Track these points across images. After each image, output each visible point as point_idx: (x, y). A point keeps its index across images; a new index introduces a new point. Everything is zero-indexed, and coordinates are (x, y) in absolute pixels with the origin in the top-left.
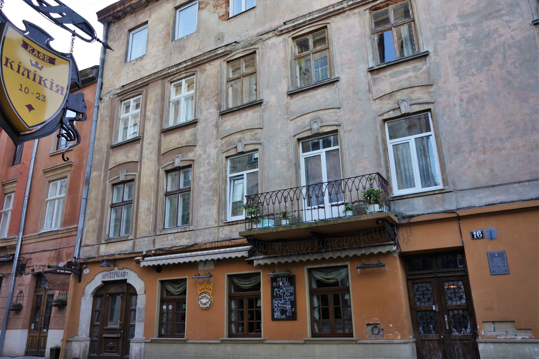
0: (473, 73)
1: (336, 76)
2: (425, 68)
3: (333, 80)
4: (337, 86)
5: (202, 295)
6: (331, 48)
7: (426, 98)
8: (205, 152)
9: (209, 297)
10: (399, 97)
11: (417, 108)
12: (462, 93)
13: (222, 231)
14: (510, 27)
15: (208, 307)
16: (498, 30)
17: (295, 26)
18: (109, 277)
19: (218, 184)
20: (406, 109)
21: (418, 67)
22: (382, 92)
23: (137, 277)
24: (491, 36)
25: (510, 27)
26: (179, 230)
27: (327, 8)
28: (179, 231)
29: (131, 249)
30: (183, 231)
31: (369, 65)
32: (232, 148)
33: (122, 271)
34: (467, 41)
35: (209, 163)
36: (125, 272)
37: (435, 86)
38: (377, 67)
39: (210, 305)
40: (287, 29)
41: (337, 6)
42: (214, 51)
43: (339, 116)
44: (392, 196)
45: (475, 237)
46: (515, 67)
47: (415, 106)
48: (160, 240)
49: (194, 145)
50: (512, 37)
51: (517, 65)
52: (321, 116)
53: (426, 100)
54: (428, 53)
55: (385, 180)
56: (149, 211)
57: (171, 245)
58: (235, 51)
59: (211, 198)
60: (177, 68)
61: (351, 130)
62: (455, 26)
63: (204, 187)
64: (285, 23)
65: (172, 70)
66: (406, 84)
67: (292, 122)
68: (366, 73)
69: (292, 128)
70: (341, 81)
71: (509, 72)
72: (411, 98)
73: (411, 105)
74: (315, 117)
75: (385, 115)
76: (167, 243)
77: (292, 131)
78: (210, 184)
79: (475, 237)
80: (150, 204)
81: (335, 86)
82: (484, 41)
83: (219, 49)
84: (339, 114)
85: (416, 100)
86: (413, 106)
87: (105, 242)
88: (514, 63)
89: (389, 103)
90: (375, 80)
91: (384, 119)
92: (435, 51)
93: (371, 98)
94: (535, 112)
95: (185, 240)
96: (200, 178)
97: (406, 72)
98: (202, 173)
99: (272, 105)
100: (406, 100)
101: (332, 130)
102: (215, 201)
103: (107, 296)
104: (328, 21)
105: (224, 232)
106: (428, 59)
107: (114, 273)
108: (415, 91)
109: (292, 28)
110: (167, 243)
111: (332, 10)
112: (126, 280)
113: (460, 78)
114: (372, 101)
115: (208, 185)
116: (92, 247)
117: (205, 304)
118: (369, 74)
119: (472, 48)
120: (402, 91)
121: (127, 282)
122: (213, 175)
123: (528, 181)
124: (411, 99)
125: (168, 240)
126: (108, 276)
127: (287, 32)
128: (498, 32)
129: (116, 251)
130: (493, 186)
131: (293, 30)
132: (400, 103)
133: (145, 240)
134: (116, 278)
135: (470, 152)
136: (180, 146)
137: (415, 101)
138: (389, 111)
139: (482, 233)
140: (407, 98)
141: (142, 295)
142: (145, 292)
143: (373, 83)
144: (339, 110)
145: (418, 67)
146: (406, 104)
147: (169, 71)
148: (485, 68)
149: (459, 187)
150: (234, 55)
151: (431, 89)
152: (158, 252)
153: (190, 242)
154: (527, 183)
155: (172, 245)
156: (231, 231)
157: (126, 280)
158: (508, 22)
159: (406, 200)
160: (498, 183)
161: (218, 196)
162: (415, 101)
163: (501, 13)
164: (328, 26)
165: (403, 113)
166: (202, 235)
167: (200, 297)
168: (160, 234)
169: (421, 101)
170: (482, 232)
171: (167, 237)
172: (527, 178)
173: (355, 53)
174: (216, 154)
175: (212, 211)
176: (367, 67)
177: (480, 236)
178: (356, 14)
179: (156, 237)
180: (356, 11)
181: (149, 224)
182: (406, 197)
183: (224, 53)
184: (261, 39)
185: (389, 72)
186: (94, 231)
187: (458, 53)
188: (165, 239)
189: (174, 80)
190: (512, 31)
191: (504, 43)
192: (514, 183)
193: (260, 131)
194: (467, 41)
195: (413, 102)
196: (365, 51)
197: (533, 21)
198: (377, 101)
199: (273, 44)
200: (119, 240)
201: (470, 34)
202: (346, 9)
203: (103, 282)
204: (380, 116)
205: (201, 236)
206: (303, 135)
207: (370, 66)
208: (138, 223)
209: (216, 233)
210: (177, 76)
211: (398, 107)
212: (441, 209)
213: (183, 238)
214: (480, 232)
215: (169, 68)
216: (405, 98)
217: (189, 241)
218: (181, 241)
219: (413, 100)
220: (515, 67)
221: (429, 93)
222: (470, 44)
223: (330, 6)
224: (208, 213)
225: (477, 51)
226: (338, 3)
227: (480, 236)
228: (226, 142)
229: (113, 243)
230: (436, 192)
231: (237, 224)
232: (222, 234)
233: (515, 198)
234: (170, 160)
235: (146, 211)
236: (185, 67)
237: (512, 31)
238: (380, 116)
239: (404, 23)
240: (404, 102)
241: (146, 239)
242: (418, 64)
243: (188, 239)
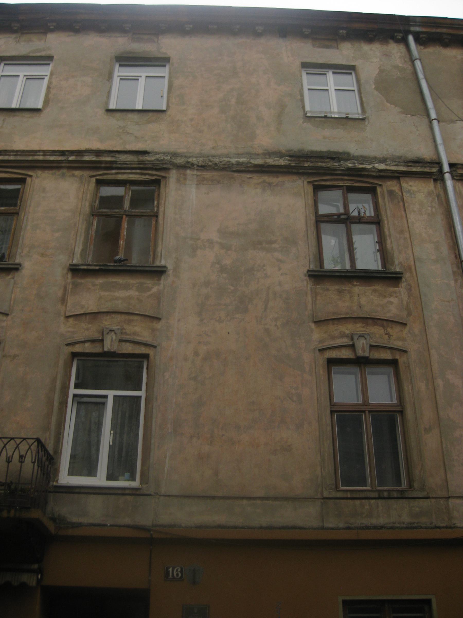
0: (220, 318)
1: (17, 261)
2: (155, 290)
3: (10, 266)
4: (13, 278)
6: (22, 214)
7: (145, 336)
10: (107, 323)
11: (128, 349)
12: (200, 343)
14: (280, 269)
16: (265, 268)
20: (111, 346)
21: (146, 285)
22: (83, 307)
24: (255, 273)
25: (280, 269)
27: (34, 152)
31: (73, 260)
34: (223, 269)
37: (163, 322)
38: (85, 267)
44: (55, 484)
45: (171, 576)
46: (276, 325)
47: (128, 344)
50: (280, 284)
51: (279, 323)
53: (145, 339)
54: (164, 269)
55: (49, 454)
61: (15, 356)
62: (211, 242)
66: (121, 306)
68: (65, 271)
70: (23, 271)
71: (267, 331)
72: (125, 329)
73: (121, 341)
75: (77, 346)
79: (171, 576)
81: (10, 277)
82: (244, 277)
85: (130, 335)
86: (124, 343)
88: (276, 320)
89: (88, 329)
90: (75, 285)
91: (74, 351)
92: (175, 270)
93: (62, 313)
94: (290, 398)
97: (126, 287)
100: (116, 331)
104: (30, 173)
106: (163, 277)
108: (133, 320)
111: (41, 158)
113: (202, 320)
114: (62, 318)
118: (70, 275)
119: (227, 281)
120: (113, 315)
123: (262, 499)
124: (124, 331)
128: (264, 270)
130: (213, 498)
132: (105, 333)
135: (192, 437)
137: (128, 337)
138: (85, 342)
139: (181, 572)
140: (118, 329)
143: (72, 288)
144: (5, 318)
145: (146, 285)
146: (114, 337)
148: (237, 316)
149: (163, 490)
151: (158, 325)
154: (259, 502)
158: (280, 261)
159: (76, 496)
160: (220, 494)
162: (128, 337)
163: (273, 246)
164: (29, 180)
165: (106, 349)
169: (138, 338)
170: (182, 569)
172: (261, 493)
173: (57, 235)
176: (70, 262)
177: (177, 575)
178: (76, 176)
180: (77, 173)
182: (77, 490)
185: (100, 281)
187: (207, 284)
190: (281, 274)
191: (269, 288)
192: (243, 498)
194: (223, 269)
195: (125, 337)
196: (73, 236)
197: (308, 271)
198: (71, 320)
201: (227, 262)
202: (63, 165)
204: (68, 345)
207: (75, 262)
211: (100, 338)
212: (127, 521)
214: (179, 570)
216: (114, 328)
219: (126, 333)
220: (276, 325)
221: (153, 330)
222: (225, 275)
223: (39, 151)
225: (232, 288)
227: (177, 575)
230: (127, 492)
233: (239, 521)
237: (281, 274)
238: (68, 345)
239: (143, 214)
240: (113, 333)
242: (148, 282)
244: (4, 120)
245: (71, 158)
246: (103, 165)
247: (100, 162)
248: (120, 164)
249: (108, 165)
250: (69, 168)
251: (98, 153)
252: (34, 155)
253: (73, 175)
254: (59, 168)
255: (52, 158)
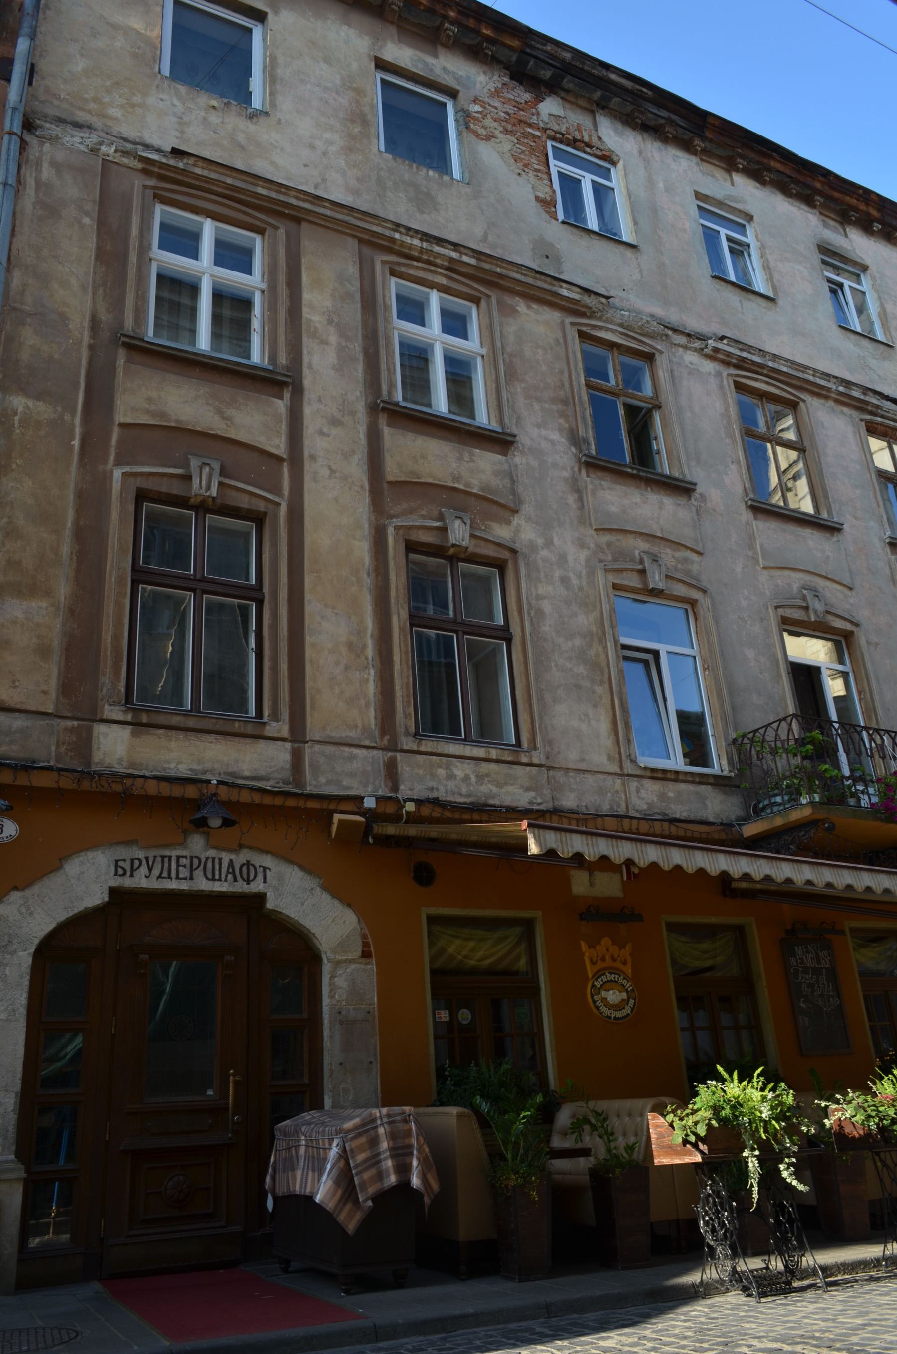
5: (604, 979)
8: (549, 544)
9: (628, 985)
13: (638, 791)
15: (628, 1015)
17: (744, 359)
18: (156, 872)
19: (600, 649)
23: (319, 889)
26: (494, 753)
28: (494, 757)
29: (287, 774)
30: (509, 759)
32: (632, 570)
33: (233, 857)
35: (564, 580)
36: (248, 864)
39: (632, 1009)
40: (728, 356)
41: (819, 377)
42: (549, 280)
43: (851, 605)
48: (421, 772)
49: (512, 505)
52: (820, 590)
56: (358, 656)
57: (466, 796)
58: (600, 319)
59: (586, 684)
60: (425, 245)
61: (876, 644)
63: (559, 645)
64: (722, 338)
65: (408, 240)
67: (766, 572)
69: (766, 587)
74: (809, 584)
76: (451, 785)
77: (767, 592)
78: (577, 642)
80: (360, 632)
81: (835, 539)
83: (564, 285)
84: (851, 601)
87: (129, 718)
95: (521, 791)
96: (540, 612)
98: (546, 600)
99: (714, 510)
101: (844, 628)
102: (601, 698)
103: (144, 957)
105: (643, 793)
107: (183, 861)
109: (737, 359)
110: (451, 785)
111: (811, 378)
112: (261, 897)
115: (570, 643)
116: (42, 723)
117: (618, 1007)
118: (888, 549)
121: (270, 905)
122: (584, 621)
125: (451, 776)
126: (150, 870)
127: (723, 362)
129: (195, 767)
131: (737, 367)
133: (352, 758)
134: (203, 884)
136: (461, 487)
141: (353, 966)
142: (366, 955)
147: (397, 236)
150: (608, 329)
152: (426, 811)
153: (539, 800)
155: (470, 796)
156: (663, 796)
157: (261, 897)
161: (607, 686)
166: (574, 786)
167: (598, 984)
168: (415, 748)
171: (448, 767)
174: (583, 564)
175: (593, 723)
178: (845, 415)
179: (399, 756)
180: (845, 410)
181: (363, 703)
183: (575, 304)
184: (667, 336)
186: (44, 651)
188: (441, 772)
189: (403, 269)
193: (694, 557)
199: (695, 367)
200: (211, 727)
203: (112, 891)
205: (572, 790)
206: (791, 614)
208: (309, 684)
209: (617, 792)
210: (417, 267)
213: (512, 785)
215: (398, 225)
217: (535, 798)
218: (503, 790)
223: (810, 368)
224: (584, 727)
226: (823, 373)
228: (609, 544)
229: (181, 734)
231: (676, 780)
232: (639, 797)
234: (423, 512)
235: (344, 650)
236: (451, 259)
241: (356, 751)
243: (528, 789)
244: (740, 301)
245: (841, 389)
246: (870, 408)
247: (867, 403)
248: (885, 411)
249: (874, 410)
250: (837, 401)
251: (866, 390)
252: (803, 372)
253: (842, 412)
254: (826, 397)
255: (823, 382)
